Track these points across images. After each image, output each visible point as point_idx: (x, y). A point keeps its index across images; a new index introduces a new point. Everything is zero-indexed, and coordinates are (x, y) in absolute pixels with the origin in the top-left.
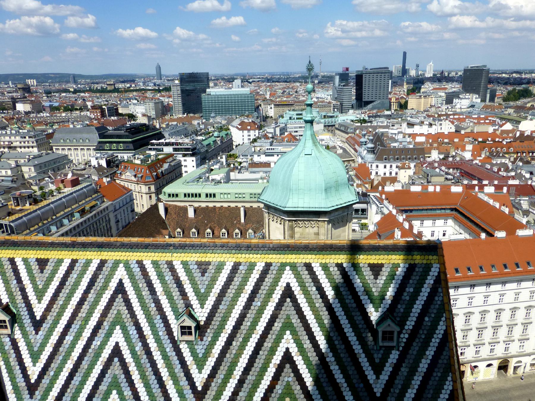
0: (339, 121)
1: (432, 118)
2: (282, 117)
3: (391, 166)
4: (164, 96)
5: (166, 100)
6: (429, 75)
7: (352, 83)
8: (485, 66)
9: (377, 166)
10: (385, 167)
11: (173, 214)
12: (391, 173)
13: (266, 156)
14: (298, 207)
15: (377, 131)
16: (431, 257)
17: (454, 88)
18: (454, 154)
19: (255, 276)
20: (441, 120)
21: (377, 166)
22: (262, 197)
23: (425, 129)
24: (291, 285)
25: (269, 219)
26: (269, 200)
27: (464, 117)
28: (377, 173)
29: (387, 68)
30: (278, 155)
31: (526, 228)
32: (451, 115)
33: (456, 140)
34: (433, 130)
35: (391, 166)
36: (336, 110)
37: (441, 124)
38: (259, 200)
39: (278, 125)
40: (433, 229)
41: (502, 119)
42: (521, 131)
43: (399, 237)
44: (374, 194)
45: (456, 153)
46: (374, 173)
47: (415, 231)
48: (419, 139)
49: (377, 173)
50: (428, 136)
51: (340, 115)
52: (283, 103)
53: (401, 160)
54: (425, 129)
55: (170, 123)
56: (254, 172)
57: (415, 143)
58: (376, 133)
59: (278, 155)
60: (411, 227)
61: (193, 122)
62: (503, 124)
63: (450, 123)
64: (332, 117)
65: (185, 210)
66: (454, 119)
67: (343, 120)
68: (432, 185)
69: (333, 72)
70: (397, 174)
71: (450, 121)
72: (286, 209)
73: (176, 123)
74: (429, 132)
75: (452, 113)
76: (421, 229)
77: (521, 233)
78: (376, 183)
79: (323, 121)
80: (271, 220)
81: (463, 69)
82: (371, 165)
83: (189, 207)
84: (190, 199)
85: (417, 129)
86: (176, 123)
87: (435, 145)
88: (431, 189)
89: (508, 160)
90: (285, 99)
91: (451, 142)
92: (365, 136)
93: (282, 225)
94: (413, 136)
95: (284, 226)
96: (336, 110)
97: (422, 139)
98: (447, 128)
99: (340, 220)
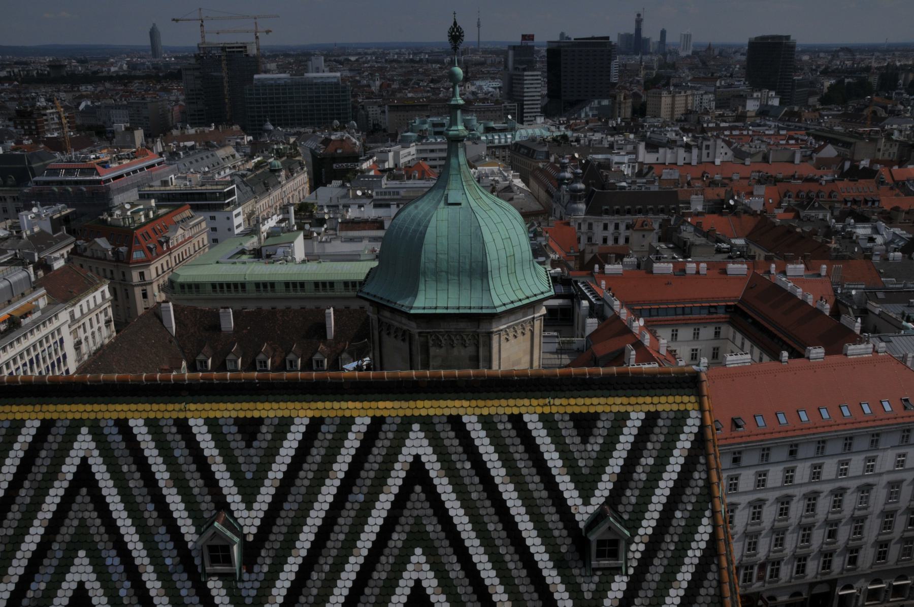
0: (517, 139)
3: (617, 226)
7: (541, 64)
8: (788, 37)
10: (606, 227)
12: (616, 240)
13: (376, 206)
15: (590, 157)
16: (686, 399)
19: (352, 443)
20: (707, 139)
22: (366, 290)
24: (424, 459)
25: (380, 333)
26: (379, 295)
27: (750, 133)
28: (590, 239)
29: (607, 38)
30: (398, 206)
32: (725, 129)
35: (617, 226)
36: (510, 117)
37: (708, 147)
38: (360, 294)
41: (817, 138)
43: (632, 361)
44: (582, 280)
45: (735, 201)
47: (663, 351)
48: (666, 174)
49: (590, 239)
51: (518, 125)
56: (351, 240)
58: (587, 161)
62: (821, 148)
63: (723, 144)
70: (627, 240)
71: (724, 140)
72: (412, 311)
75: (727, 125)
78: (588, 257)
80: (384, 334)
81: (746, 42)
83: (221, 310)
90: (410, 95)
92: (566, 167)
93: (407, 344)
95: (410, 344)
96: (510, 117)
97: (675, 175)
99: (519, 332)
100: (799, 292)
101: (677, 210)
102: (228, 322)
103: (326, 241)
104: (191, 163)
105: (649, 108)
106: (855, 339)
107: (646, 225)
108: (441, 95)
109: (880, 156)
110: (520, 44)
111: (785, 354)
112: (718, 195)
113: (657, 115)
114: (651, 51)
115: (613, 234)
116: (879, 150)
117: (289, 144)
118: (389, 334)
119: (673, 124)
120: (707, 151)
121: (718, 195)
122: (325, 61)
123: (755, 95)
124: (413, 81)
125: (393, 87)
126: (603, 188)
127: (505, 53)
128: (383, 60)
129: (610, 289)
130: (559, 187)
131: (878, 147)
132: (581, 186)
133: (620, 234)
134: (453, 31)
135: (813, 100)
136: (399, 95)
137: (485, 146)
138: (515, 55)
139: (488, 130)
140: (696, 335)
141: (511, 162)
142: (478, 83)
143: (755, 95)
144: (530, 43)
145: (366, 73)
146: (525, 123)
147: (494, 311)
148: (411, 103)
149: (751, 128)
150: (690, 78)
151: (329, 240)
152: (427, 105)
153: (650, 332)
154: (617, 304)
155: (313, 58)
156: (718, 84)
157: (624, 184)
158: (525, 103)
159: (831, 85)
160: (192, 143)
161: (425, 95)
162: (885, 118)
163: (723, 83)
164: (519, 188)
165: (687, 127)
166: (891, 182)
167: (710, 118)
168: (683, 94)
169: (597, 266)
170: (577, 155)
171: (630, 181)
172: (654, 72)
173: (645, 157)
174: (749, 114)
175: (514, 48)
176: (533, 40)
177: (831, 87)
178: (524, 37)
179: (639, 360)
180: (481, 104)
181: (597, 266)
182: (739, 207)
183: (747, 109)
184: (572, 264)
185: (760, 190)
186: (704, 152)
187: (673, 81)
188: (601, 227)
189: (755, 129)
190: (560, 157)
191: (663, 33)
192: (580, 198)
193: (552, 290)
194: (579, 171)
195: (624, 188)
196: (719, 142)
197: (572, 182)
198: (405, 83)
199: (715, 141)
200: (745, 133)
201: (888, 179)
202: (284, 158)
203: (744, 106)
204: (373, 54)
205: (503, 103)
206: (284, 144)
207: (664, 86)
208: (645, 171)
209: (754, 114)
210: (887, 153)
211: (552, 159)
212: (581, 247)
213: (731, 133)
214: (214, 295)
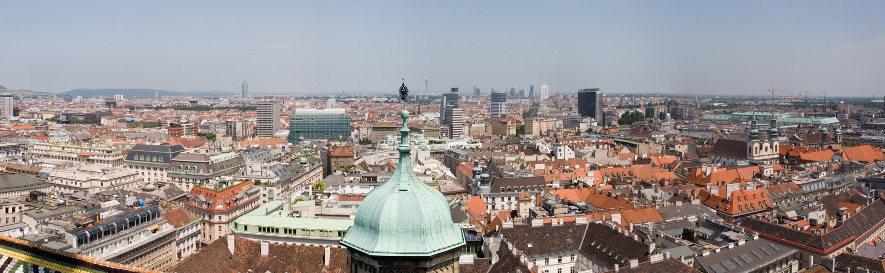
0: (449, 148)
10: (503, 199)
11: (243, 250)
18: (576, 182)
28: (493, 207)
33: (577, 166)
37: (560, 150)
49: (493, 207)
52: (383, 126)
56: (346, 206)
57: (534, 171)
62: (621, 149)
63: (569, 148)
64: (440, 143)
65: (259, 246)
66: (573, 144)
67: (454, 147)
78: (493, 218)
79: (429, 147)
81: (575, 91)
84: (266, 234)
90: (385, 121)
92: (478, 164)
96: (444, 135)
101: (545, 187)
103: (330, 207)
104: (256, 157)
105: (526, 130)
107: (527, 197)
110: (450, 93)
112: (568, 178)
113: (531, 133)
114: (526, 96)
115: (507, 203)
117: (312, 148)
119: (540, 137)
121: (568, 178)
122: (337, 101)
123: (584, 120)
126: (501, 177)
127: (442, 98)
128: (371, 101)
130: (474, 176)
131: (650, 147)
132: (486, 175)
133: (511, 203)
135: (615, 123)
136: (379, 121)
138: (447, 99)
139: (431, 142)
141: (445, 161)
142: (426, 115)
143: (584, 120)
145: (360, 109)
146: (453, 138)
148: (386, 126)
150: (548, 112)
152: (395, 128)
155: (329, 100)
156: (564, 114)
157: (512, 173)
158: (453, 126)
159: (623, 114)
160: (258, 145)
161: (394, 121)
162: (651, 132)
163: (567, 114)
165: (548, 139)
166: (659, 165)
168: (545, 120)
170: (484, 157)
171: (516, 172)
172: (528, 108)
174: (581, 131)
175: (446, 95)
176: (457, 91)
177: (623, 115)
178: (454, 90)
182: (580, 184)
183: (581, 128)
184: (483, 222)
185: (591, 173)
187: (539, 113)
188: (500, 199)
189: (587, 139)
190: (474, 158)
191: (532, 87)
192: (487, 182)
194: (485, 166)
195: (512, 176)
196: (566, 147)
197: (482, 173)
199: (564, 147)
200: (580, 141)
201: (657, 163)
202: (309, 157)
203: (579, 127)
204: (365, 97)
205: (440, 126)
206: (309, 148)
207: (534, 116)
208: (525, 165)
209: (584, 131)
210: (655, 150)
211: (469, 160)
212: (488, 212)
214: (260, 234)
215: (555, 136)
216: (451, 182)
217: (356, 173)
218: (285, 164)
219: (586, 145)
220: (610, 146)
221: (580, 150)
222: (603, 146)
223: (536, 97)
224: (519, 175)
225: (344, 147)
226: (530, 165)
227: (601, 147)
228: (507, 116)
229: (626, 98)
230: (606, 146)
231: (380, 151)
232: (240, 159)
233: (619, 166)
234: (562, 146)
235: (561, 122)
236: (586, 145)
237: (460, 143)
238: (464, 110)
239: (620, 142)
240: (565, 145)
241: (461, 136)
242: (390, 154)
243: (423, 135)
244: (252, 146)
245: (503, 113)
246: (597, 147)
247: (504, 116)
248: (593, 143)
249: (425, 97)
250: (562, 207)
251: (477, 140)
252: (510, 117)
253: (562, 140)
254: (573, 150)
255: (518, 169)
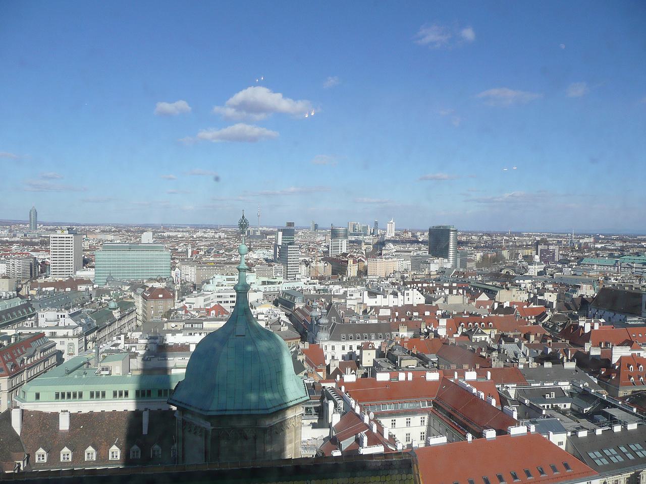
1: (396, 287)
2: (208, 283)
4: (37, 251)
5: (41, 256)
6: (390, 235)
9: (333, 348)
14: (226, 410)
17: (420, 250)
18: (426, 331)
20: (408, 289)
21: (333, 348)
23: (391, 301)
28: (333, 357)
30: (200, 334)
31: (519, 425)
33: (427, 313)
34: (399, 301)
37: (408, 294)
39: (202, 292)
40: (408, 430)
42: (499, 303)
46: (329, 358)
47: (386, 436)
49: (333, 357)
50: (395, 309)
53: (362, 339)
54: (391, 301)
55: (44, 289)
59: (200, 334)
60: (381, 429)
61: (79, 287)
66: (422, 287)
68: (403, 371)
69: (274, 227)
73: (53, 288)
74: (395, 304)
76: (393, 432)
77: (515, 431)
78: (332, 370)
79: (262, 288)
82: (326, 346)
85: (379, 301)
86: (53, 288)
87: (403, 320)
88: (402, 376)
89: (488, 337)
90: (212, 259)
91: (422, 315)
94: (377, 309)
95: (206, 438)
97: (388, 313)
98: (415, 298)
100: (475, 391)
102: (64, 424)
106: (515, 423)
108: (233, 260)
109: (514, 300)
111: (470, 437)
116: (514, 296)
118: (190, 431)
120: (408, 297)
123: (435, 261)
124: (214, 250)
125: (200, 253)
129: (347, 392)
134: (242, 222)
137: (262, 294)
140: (408, 423)
144: (292, 228)
147: (267, 412)
149: (434, 282)
151: (149, 359)
153: (376, 422)
154: (353, 402)
164: (284, 322)
167: (408, 275)
169: (338, 376)
173: (370, 302)
179: (370, 444)
180: (259, 266)
181: (338, 376)
185: (443, 322)
186: (406, 297)
187: (384, 252)
189: (438, 283)
193: (308, 396)
198: (208, 252)
200: (431, 285)
203: (429, 268)
208: (368, 310)
213: (422, 285)
215: (403, 278)
216: (286, 328)
217: (178, 319)
218: (90, 310)
219: (438, 289)
220: (465, 291)
221: (430, 295)
222: (458, 291)
223: (381, 235)
224: (362, 321)
225: (162, 289)
226: (374, 310)
227: (455, 292)
228: (349, 255)
229: (485, 237)
230: (461, 291)
231: (205, 293)
232: (28, 305)
233: (475, 315)
234: (410, 290)
235: (409, 262)
236: (438, 289)
237: (295, 285)
238: (300, 248)
239: (477, 287)
240: (413, 288)
241: (298, 276)
242: (219, 297)
243: (255, 274)
244: (44, 289)
245: (344, 251)
246: (451, 292)
247: (345, 255)
248: (446, 288)
249: (257, 233)
250: (410, 359)
251: (315, 281)
252: (352, 256)
253: (410, 283)
254: (422, 294)
255: (361, 314)
